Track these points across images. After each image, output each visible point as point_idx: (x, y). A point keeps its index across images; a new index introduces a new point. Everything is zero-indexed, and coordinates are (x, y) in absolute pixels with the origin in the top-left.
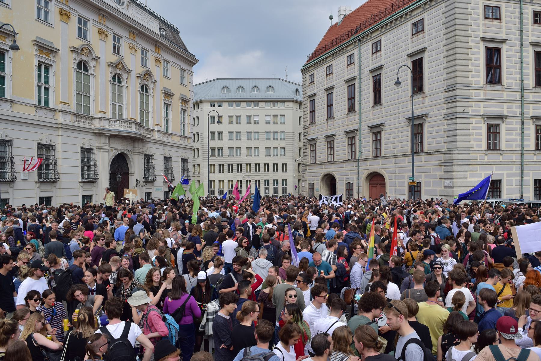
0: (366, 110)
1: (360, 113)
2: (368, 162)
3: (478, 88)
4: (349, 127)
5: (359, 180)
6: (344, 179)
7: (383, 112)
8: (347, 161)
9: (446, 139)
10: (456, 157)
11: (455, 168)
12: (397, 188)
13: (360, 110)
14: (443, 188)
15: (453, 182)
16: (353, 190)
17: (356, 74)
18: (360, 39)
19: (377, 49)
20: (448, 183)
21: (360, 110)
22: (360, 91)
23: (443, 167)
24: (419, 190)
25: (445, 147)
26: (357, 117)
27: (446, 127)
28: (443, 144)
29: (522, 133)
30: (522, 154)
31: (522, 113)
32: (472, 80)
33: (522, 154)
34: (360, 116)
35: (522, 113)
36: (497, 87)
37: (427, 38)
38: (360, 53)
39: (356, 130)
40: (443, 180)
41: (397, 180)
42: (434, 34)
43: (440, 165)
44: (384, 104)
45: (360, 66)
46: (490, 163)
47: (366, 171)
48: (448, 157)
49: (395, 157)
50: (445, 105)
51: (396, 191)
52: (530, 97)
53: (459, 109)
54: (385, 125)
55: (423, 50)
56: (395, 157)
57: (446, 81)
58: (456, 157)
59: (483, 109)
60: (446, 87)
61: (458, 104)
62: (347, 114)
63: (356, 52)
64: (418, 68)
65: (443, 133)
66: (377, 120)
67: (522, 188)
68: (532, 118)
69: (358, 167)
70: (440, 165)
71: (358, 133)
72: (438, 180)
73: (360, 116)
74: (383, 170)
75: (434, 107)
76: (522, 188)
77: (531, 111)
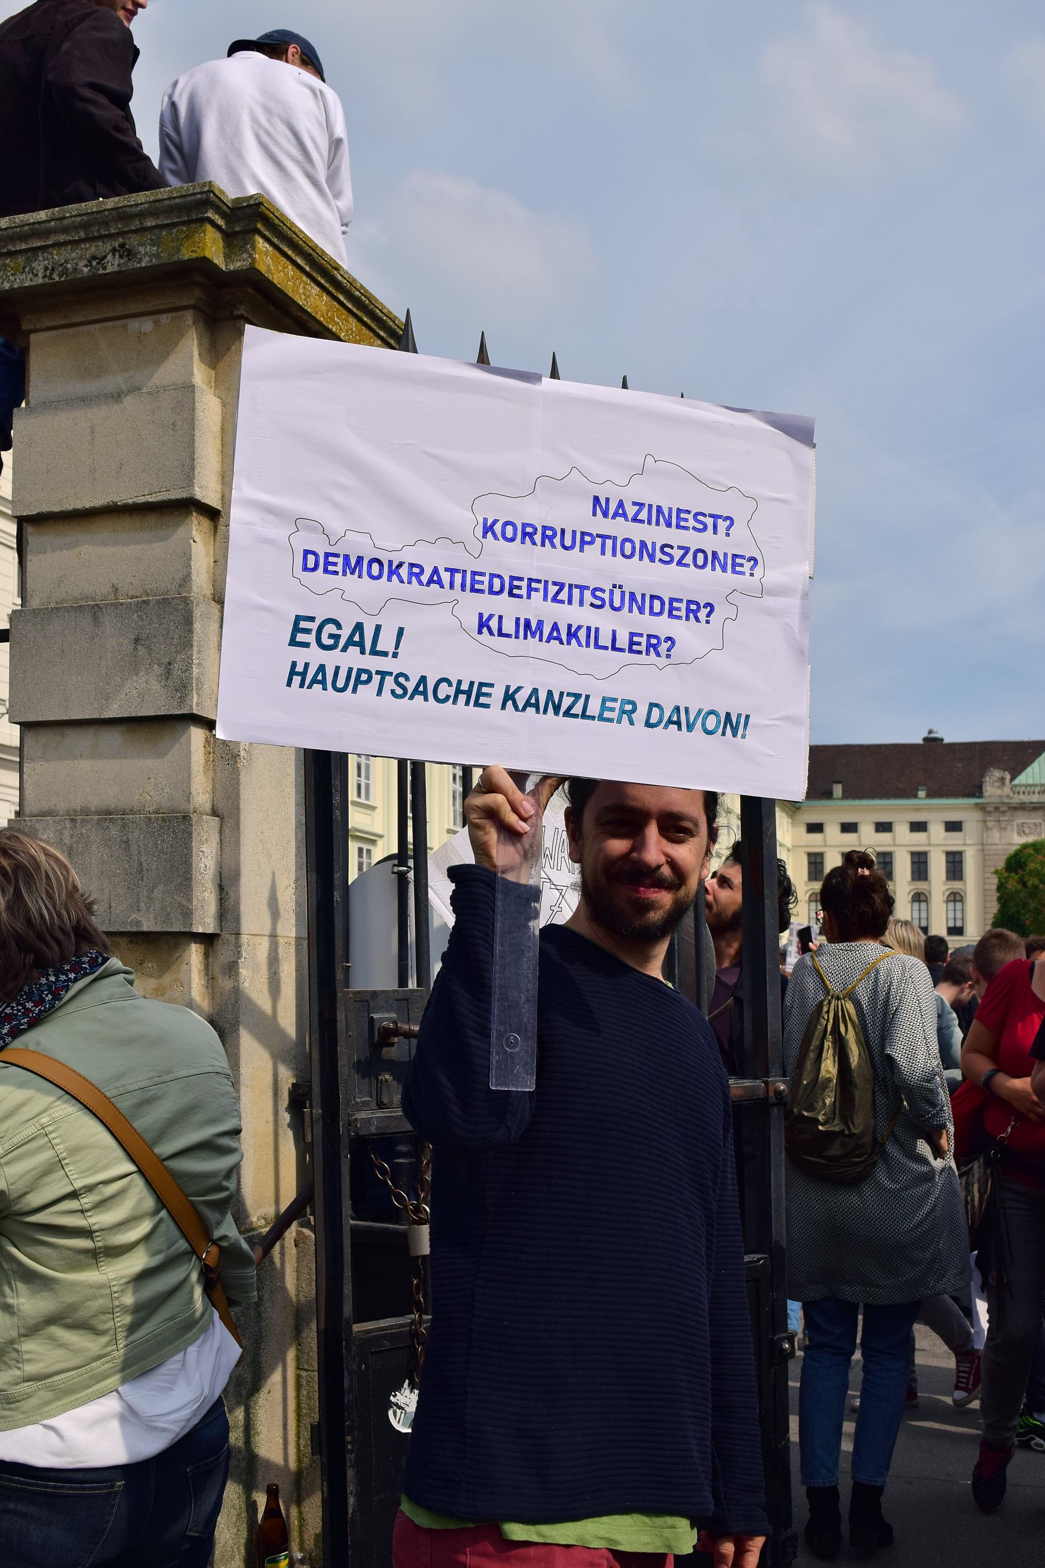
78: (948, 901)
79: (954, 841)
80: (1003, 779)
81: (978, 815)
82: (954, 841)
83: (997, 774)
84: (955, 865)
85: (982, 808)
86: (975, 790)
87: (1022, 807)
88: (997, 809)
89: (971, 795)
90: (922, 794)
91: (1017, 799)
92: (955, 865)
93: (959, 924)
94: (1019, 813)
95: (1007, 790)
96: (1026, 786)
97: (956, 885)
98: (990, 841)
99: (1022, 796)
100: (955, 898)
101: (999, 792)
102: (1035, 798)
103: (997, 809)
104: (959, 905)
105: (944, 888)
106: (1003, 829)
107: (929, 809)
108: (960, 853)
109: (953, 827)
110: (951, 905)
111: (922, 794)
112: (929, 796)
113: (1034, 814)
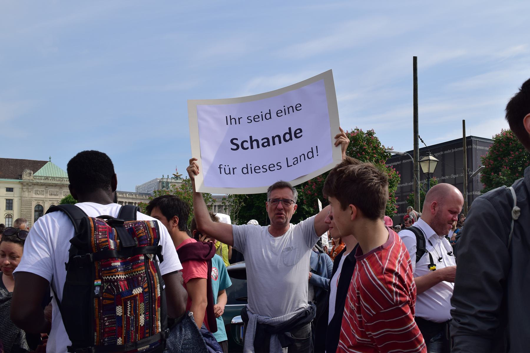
80: (30, 173)
81: (20, 186)
83: (28, 171)
85: (22, 183)
86: (20, 177)
87: (37, 184)
88: (27, 184)
89: (18, 179)
91: (35, 181)
94: (36, 186)
95: (32, 178)
96: (39, 176)
97: (10, 212)
98: (24, 196)
99: (37, 180)
101: (29, 178)
102: (42, 181)
103: (27, 184)
105: (5, 213)
106: (29, 192)
108: (12, 200)
109: (10, 190)
110: (7, 219)
113: (42, 187)
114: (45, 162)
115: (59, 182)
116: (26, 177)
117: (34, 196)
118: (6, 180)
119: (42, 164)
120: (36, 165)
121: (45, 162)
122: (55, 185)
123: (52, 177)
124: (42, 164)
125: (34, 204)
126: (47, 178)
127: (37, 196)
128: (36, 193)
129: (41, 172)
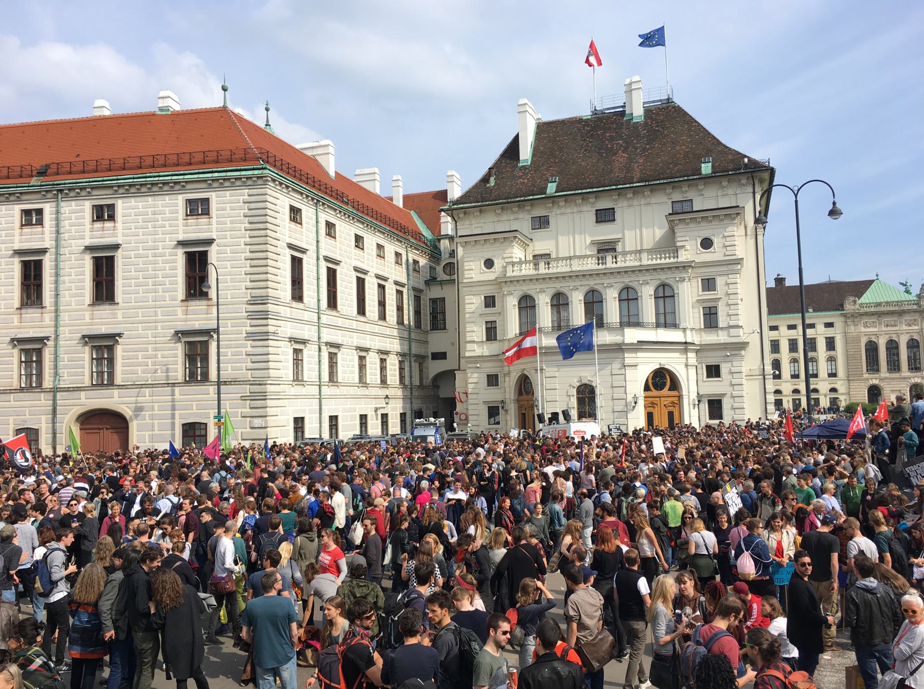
0: (74, 307)
1: (56, 311)
2: (83, 394)
3: (285, 305)
4: (22, 330)
5: (54, 422)
6: (11, 421)
7: (120, 318)
8: (15, 391)
9: (250, 365)
10: (270, 388)
11: (270, 403)
12: (156, 432)
13: (56, 303)
14: (249, 430)
15: (266, 422)
16: (37, 440)
17: (46, 244)
18: (61, 191)
19: (104, 214)
20: (257, 422)
21: (56, 303)
22: (57, 275)
23: (248, 402)
24: (203, 432)
25: (249, 375)
26: (48, 318)
27: (249, 349)
28: (244, 371)
29: (320, 361)
30: (320, 386)
31: (319, 338)
32: (279, 294)
33: (320, 386)
34: (57, 317)
35: (319, 338)
36: (300, 305)
37: (215, 226)
38: (58, 212)
39: (47, 338)
40: (248, 419)
41: (156, 422)
42: (229, 225)
43: (243, 398)
44: (121, 304)
45: (58, 232)
46: (296, 397)
47: (76, 408)
48: (256, 388)
49: (152, 386)
50: (249, 321)
51: (151, 434)
52: (324, 319)
53: (271, 329)
54: (124, 336)
55: (210, 242)
56: (152, 386)
57: (249, 291)
58: (270, 388)
59: (288, 329)
60: (249, 298)
61: (270, 322)
62: (20, 309)
63: (48, 209)
64: (197, 265)
65: (244, 356)
66: (103, 327)
67: (320, 427)
68: (327, 344)
69: (54, 400)
70: (243, 398)
71: (50, 343)
72: (240, 418)
73: (57, 317)
74: (123, 407)
75: (229, 322)
76: (320, 427)
77: (327, 335)
78: (828, 360)
79: (830, 332)
81: (843, 319)
82: (830, 332)
83: (852, 299)
84: (831, 344)
85: (845, 316)
86: (841, 307)
88: (852, 316)
90: (811, 310)
91: (862, 311)
92: (831, 344)
93: (834, 371)
95: (857, 306)
97: (832, 353)
100: (831, 359)
102: (872, 309)
103: (852, 316)
104: (833, 363)
106: (855, 325)
107: (817, 317)
108: (833, 338)
109: (829, 325)
111: (811, 310)
112: (814, 311)
114: (871, 282)
115: (897, 308)
116: (849, 307)
117: (863, 329)
118: (823, 313)
119: (867, 284)
120: (860, 287)
121: (871, 282)
122: (892, 313)
123: (886, 303)
124: (867, 284)
125: (864, 341)
126: (879, 304)
127: (868, 330)
128: (866, 326)
129: (868, 297)
